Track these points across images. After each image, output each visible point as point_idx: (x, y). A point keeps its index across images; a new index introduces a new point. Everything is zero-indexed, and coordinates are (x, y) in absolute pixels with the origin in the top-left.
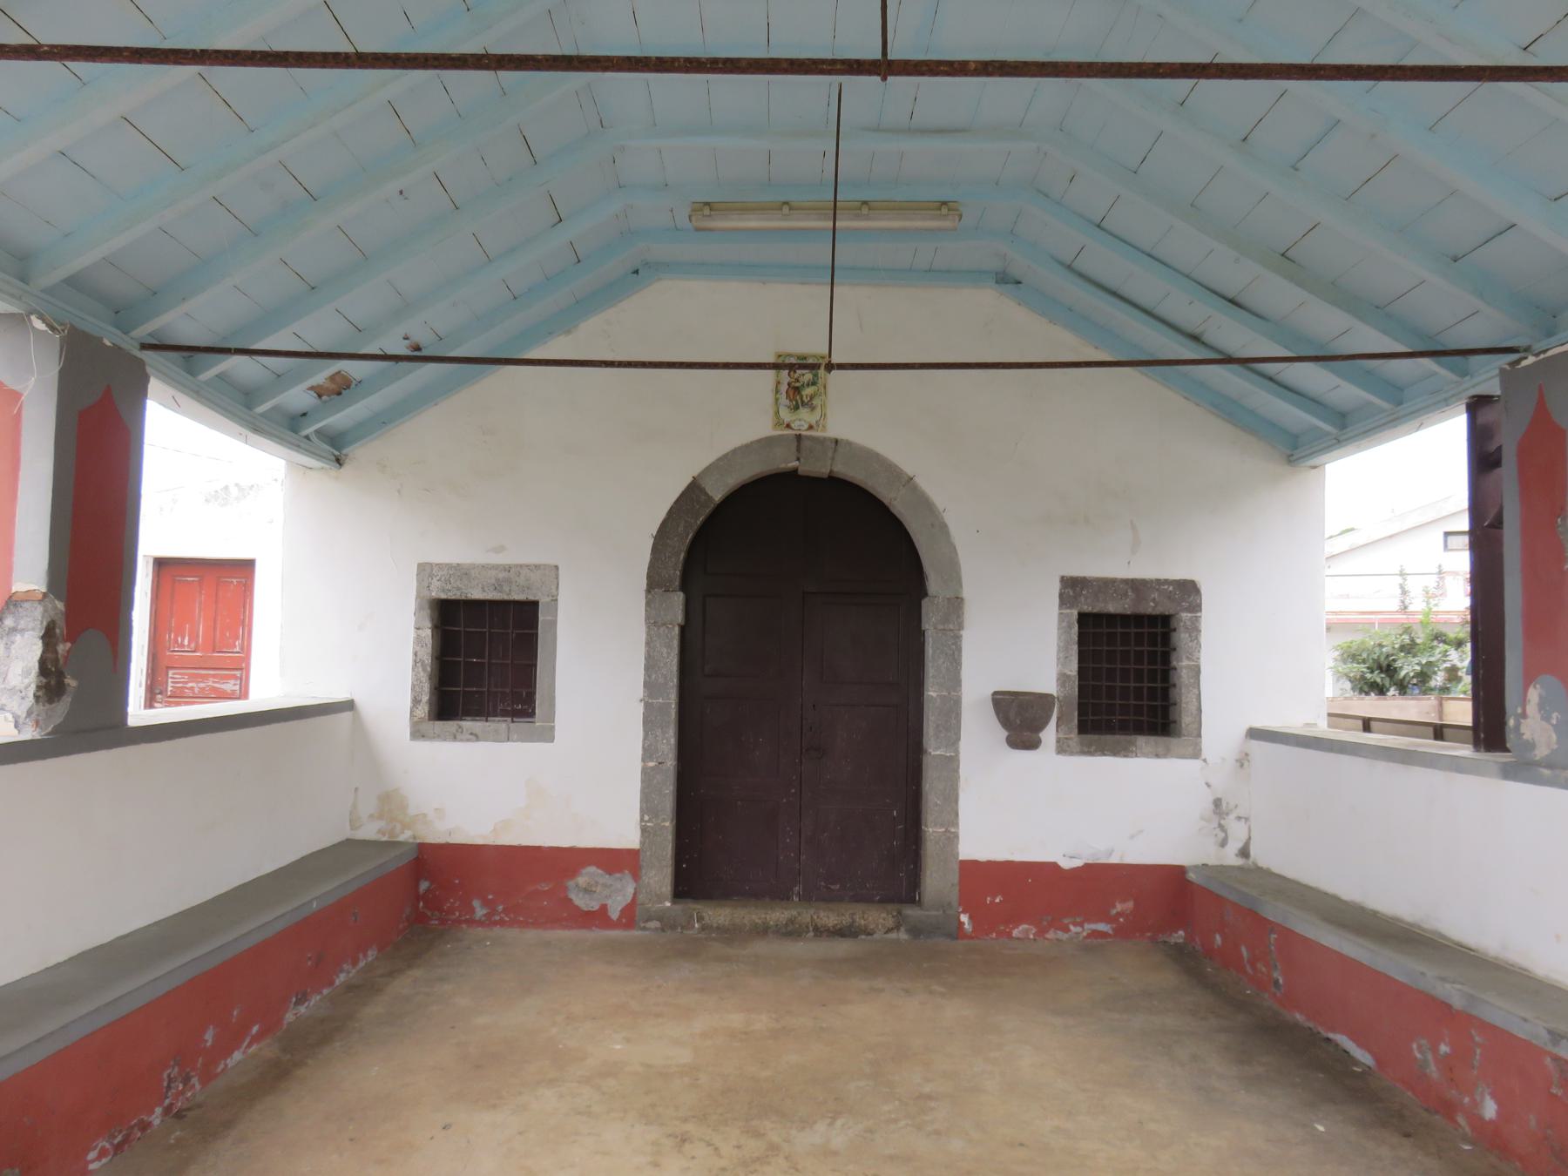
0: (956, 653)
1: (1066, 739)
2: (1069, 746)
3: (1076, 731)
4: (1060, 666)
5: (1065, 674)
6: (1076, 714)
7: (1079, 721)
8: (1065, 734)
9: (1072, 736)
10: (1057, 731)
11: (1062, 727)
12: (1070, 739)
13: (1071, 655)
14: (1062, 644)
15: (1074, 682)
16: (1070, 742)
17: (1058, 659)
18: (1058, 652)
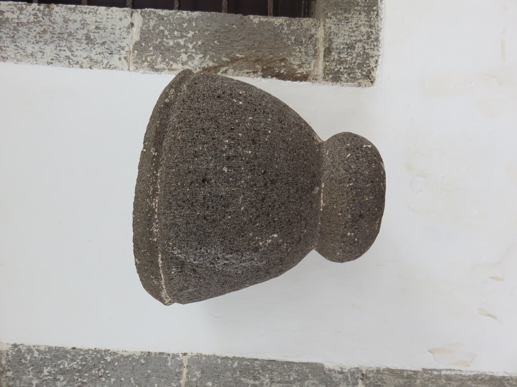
0: (66, 365)
1: (328, 51)
2: (351, 47)
3: (306, 22)
4: (114, 60)
5: (137, 45)
6: (256, 19)
7: (276, 14)
8: (315, 55)
9: (320, 34)
10: (304, 78)
11: (295, 62)
12: (329, 40)
13: (84, 24)
14: (50, 50)
15: (161, 18)
16: (338, 42)
17: (93, 64)
18: (70, 62)
